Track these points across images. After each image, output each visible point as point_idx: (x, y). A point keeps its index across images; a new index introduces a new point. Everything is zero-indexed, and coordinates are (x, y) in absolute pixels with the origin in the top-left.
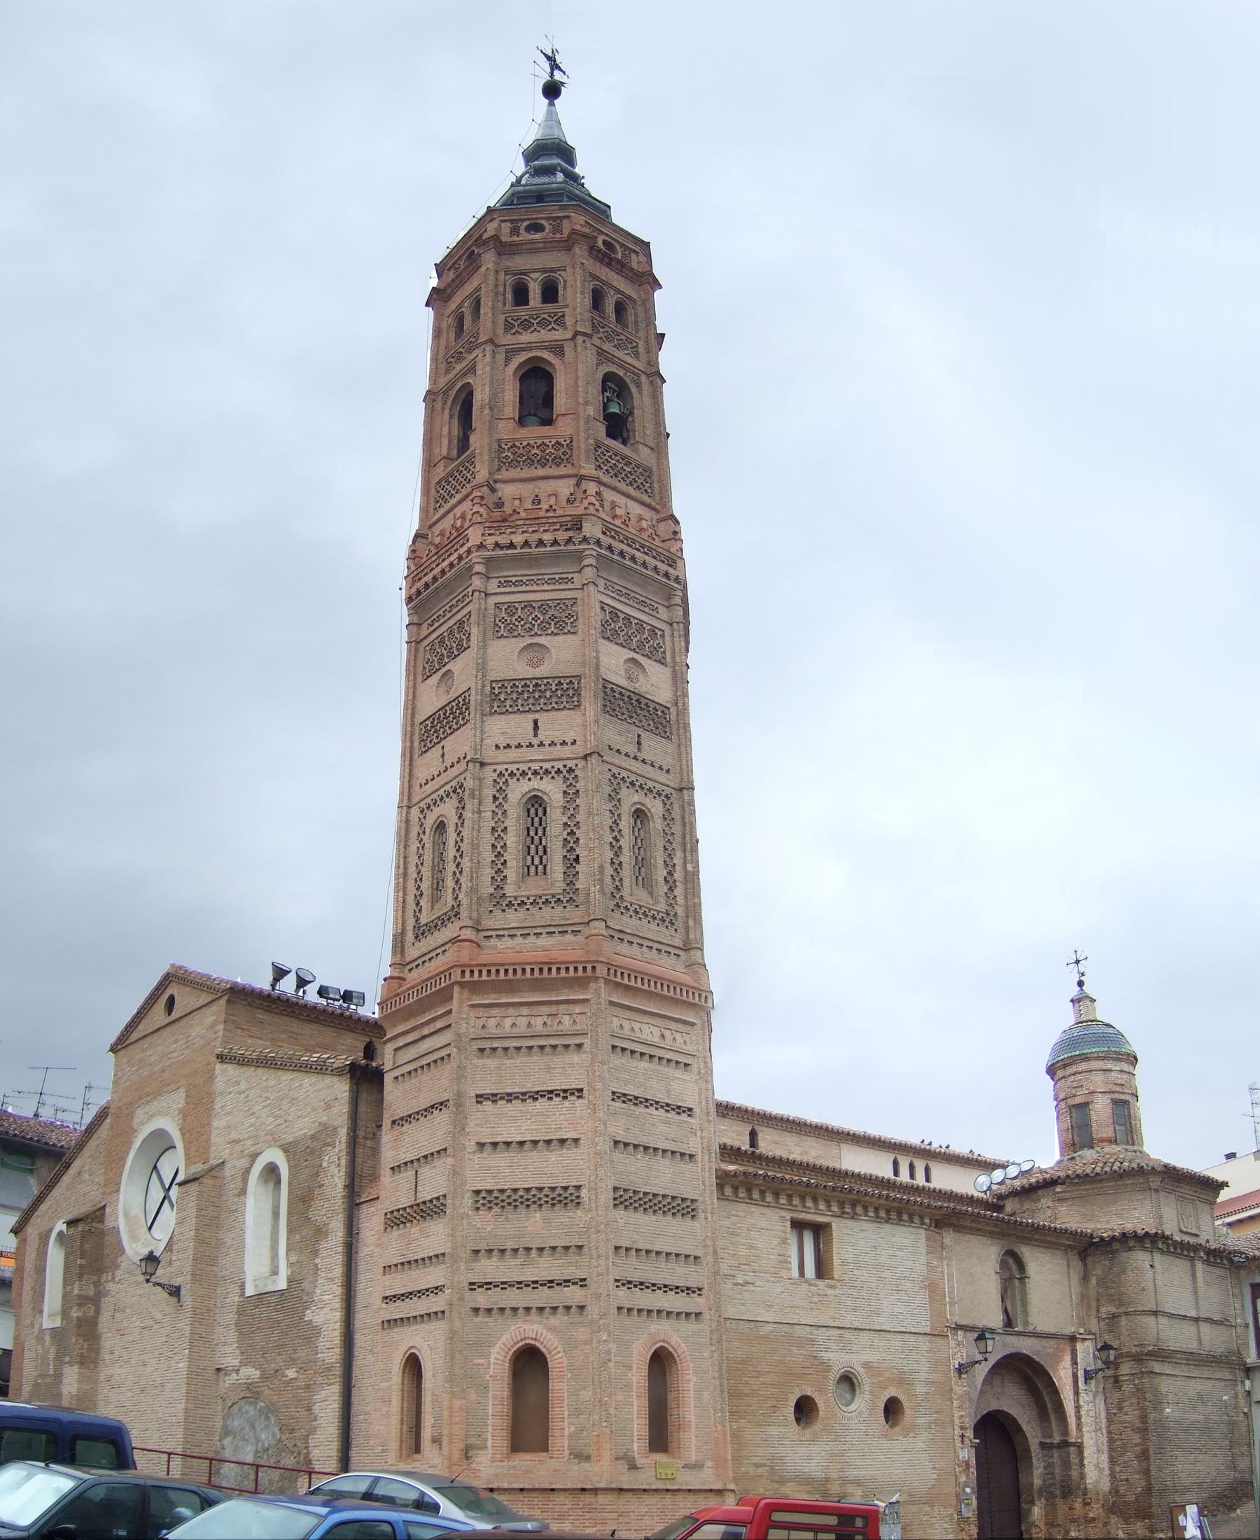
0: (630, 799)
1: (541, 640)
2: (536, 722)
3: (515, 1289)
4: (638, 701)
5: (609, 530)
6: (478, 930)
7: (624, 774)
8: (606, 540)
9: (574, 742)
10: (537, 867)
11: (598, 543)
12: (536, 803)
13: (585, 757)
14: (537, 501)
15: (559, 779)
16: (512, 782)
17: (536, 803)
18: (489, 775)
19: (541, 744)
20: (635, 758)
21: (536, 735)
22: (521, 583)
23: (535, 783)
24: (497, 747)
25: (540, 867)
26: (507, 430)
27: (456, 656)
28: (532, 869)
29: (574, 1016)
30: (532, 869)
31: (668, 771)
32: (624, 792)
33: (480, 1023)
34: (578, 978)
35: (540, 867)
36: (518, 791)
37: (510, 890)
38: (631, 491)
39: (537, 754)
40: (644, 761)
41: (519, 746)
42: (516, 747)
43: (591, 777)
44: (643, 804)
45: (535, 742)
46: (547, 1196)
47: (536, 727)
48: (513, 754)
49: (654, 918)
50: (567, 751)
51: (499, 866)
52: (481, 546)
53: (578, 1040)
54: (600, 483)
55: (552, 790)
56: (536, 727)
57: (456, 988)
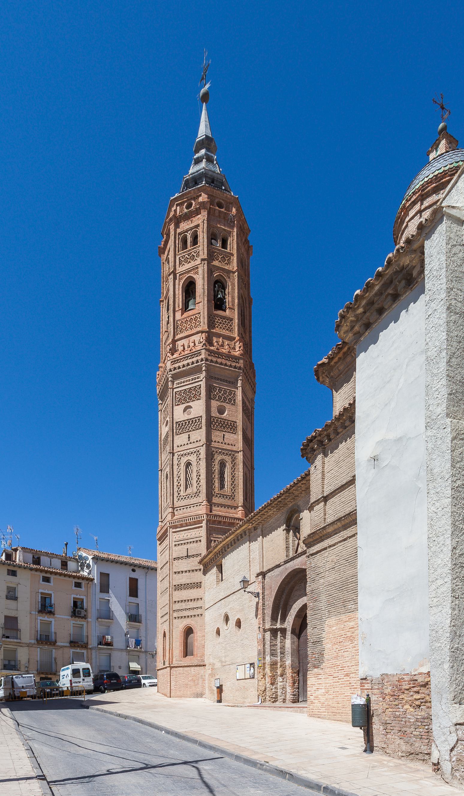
9: (200, 441)
10: (190, 485)
13: (202, 446)
25: (191, 485)
28: (188, 486)
35: (191, 485)
36: (184, 460)
37: (182, 493)
55: (193, 458)
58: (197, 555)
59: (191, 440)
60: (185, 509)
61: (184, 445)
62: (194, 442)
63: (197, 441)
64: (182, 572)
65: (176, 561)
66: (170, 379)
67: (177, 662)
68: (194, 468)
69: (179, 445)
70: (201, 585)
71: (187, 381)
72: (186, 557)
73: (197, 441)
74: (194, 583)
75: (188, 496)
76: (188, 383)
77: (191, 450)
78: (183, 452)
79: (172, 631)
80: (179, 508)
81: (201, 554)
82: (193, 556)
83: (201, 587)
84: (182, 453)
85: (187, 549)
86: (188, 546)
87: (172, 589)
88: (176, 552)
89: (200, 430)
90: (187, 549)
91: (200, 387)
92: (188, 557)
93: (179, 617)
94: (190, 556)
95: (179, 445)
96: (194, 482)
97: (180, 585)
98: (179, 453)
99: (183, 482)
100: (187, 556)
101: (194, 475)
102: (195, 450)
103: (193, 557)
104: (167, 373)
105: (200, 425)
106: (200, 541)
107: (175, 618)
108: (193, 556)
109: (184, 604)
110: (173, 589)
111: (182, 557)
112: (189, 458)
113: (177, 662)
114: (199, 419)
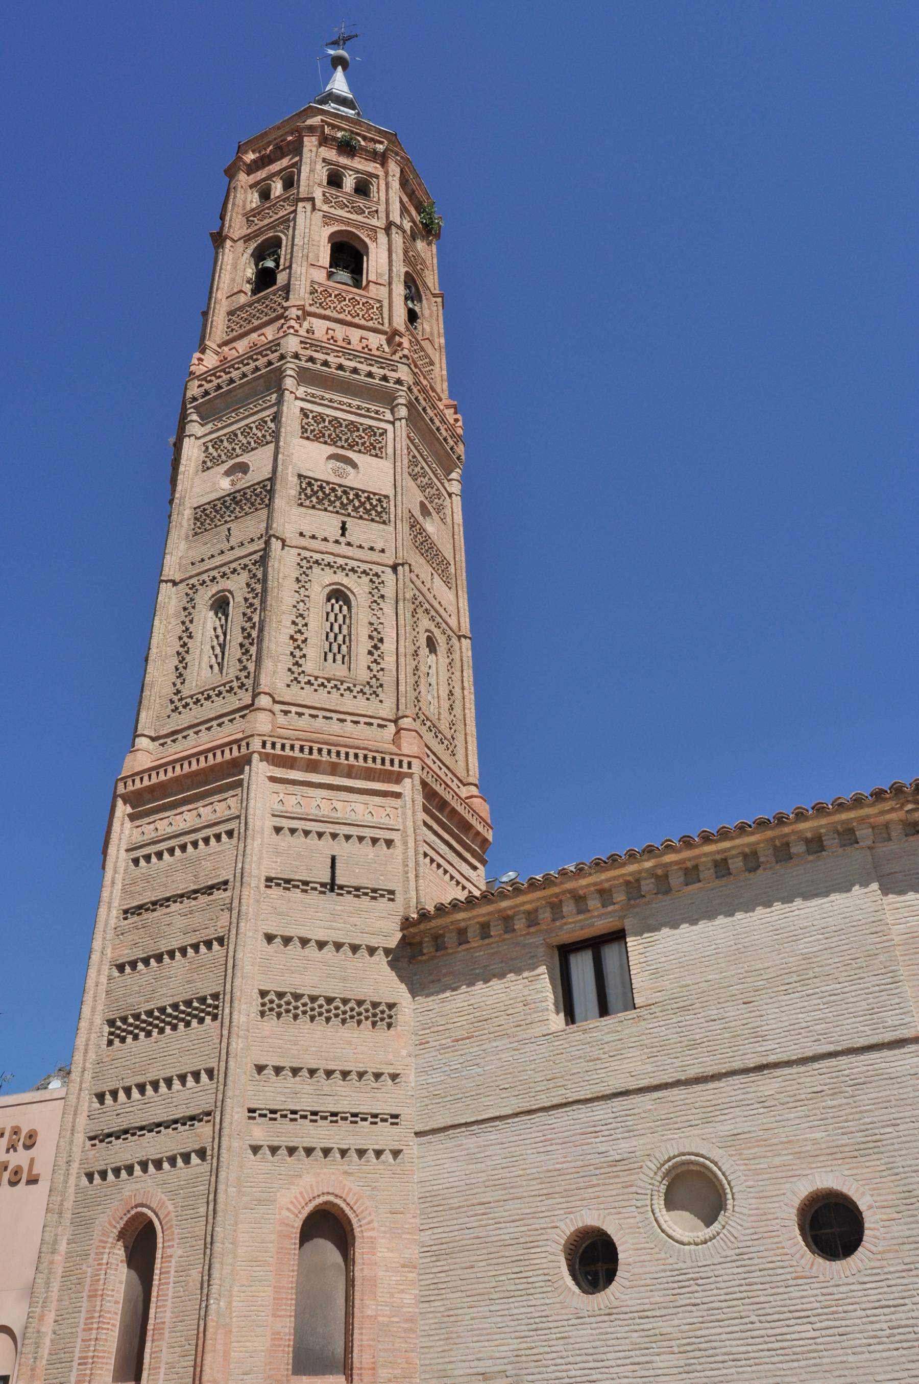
3: (308, 1121)
6: (275, 702)
9: (383, 551)
11: (409, 389)
15: (365, 579)
16: (316, 570)
21: (343, 535)
23: (340, 577)
24: (301, 534)
27: (253, 449)
39: (343, 549)
41: (325, 540)
42: (322, 540)
45: (342, 540)
46: (337, 1008)
47: (344, 528)
50: (374, 557)
59: (349, 537)
64: (304, 942)
65: (276, 892)
72: (323, 885)
82: (357, 891)
85: (333, 859)
86: (341, 849)
90: (333, 859)
92: (332, 890)
93: (274, 1150)
94: (341, 887)
100: (332, 886)
107: (255, 1149)
108: (357, 891)
109: (308, 1088)
111: (306, 883)
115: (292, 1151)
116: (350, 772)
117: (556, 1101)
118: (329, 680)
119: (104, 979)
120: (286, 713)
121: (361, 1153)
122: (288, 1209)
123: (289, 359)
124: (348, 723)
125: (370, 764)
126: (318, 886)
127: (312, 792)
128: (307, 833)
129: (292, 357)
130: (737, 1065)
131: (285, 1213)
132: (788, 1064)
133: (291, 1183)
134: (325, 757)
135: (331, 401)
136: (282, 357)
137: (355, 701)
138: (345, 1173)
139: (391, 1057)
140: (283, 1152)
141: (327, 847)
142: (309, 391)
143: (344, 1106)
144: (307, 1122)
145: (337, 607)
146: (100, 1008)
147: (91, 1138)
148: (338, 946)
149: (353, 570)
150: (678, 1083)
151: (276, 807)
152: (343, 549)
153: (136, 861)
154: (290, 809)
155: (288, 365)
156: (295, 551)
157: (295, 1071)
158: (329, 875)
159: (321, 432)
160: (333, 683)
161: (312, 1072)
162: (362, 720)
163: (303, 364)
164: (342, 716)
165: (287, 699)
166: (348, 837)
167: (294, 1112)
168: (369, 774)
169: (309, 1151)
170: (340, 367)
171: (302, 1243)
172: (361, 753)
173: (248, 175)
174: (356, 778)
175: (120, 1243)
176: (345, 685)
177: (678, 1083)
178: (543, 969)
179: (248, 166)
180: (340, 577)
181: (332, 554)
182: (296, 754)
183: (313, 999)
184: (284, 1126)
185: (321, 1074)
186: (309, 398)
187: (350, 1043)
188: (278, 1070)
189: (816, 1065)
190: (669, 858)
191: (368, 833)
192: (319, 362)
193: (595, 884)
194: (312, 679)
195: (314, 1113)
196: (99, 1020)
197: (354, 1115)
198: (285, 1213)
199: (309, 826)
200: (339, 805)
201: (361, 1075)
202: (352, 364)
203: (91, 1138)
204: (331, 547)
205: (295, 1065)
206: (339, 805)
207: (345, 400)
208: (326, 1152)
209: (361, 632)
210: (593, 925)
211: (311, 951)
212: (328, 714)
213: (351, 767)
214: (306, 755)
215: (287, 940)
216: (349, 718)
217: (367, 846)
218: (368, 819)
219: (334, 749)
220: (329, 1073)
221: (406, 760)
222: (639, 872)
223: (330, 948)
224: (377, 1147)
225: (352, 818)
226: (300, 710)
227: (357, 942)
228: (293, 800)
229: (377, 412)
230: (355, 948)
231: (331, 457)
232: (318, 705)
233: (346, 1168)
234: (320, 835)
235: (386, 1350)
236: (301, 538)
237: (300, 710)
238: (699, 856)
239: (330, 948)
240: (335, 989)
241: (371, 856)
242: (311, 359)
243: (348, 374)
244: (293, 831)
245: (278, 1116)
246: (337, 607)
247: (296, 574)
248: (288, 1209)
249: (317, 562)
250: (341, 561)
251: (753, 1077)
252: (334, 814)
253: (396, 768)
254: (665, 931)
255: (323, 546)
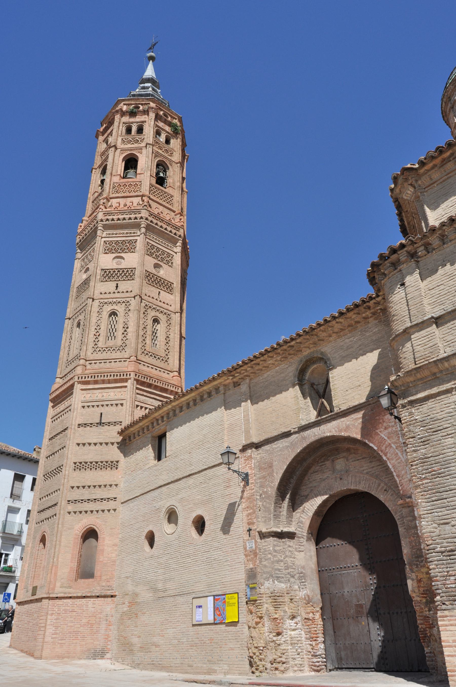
0: (152, 314)
1: (122, 255)
2: (117, 284)
4: (160, 280)
5: (152, 215)
6: (86, 360)
7: (151, 305)
8: (150, 218)
9: (131, 291)
11: (147, 219)
12: (113, 314)
13: (134, 297)
14: (125, 205)
17: (113, 314)
18: (96, 303)
19: (119, 292)
20: (156, 299)
21: (117, 289)
22: (116, 234)
24: (101, 293)
26: (116, 179)
28: (110, 338)
29: (122, 392)
30: (110, 338)
31: (171, 306)
32: (149, 310)
33: (83, 396)
34: (123, 379)
35: (113, 337)
36: (108, 309)
38: (164, 203)
39: (117, 295)
40: (160, 301)
43: (134, 303)
44: (157, 316)
47: (117, 287)
48: (107, 296)
49: (159, 358)
51: (97, 336)
52: (102, 220)
53: (121, 402)
54: (150, 199)
55: (120, 309)
56: (117, 287)
57: (76, 383)
58: (115, 423)
59: (119, 289)
60: (103, 364)
61: (110, 293)
62: (123, 292)
63: (127, 292)
64: (90, 444)
65: (82, 428)
66: (99, 228)
67: (61, 590)
68: (121, 319)
69: (103, 293)
70: (117, 465)
71: (120, 234)
72: (97, 424)
73: (127, 292)
74: (107, 462)
75: (108, 349)
76: (121, 235)
77: (119, 300)
78: (108, 300)
79: (61, 536)
80: (93, 362)
81: (121, 422)
82: (109, 424)
83: (117, 468)
84: (106, 301)
85: (101, 414)
86: (104, 410)
87: (70, 467)
88: (82, 415)
89: (131, 281)
90: (101, 414)
91: (136, 242)
92: (100, 425)
93: (75, 512)
94: (103, 423)
95: (103, 293)
96: (119, 335)
97: (85, 462)
98: (102, 301)
99: (103, 332)
100: (101, 423)
101: (120, 327)
102: (124, 300)
103: (109, 426)
104: (97, 222)
105: (133, 276)
106: (122, 405)
107: (69, 513)
108: (109, 424)
109: (87, 492)
110: (71, 469)
111: (91, 424)
112: (115, 307)
113: (61, 590)
114: (132, 271)
115: (81, 512)
116: (109, 382)
117: (148, 490)
118: (107, 348)
119: (43, 462)
120: (90, 364)
121: (103, 511)
122: (78, 530)
123: (99, 223)
124: (113, 363)
125: (115, 377)
126: (96, 424)
127: (95, 391)
128: (93, 406)
129: (100, 221)
130: (185, 475)
131: (77, 532)
132: (196, 473)
133: (79, 522)
134: (99, 378)
135: (116, 234)
136: (97, 222)
137: (116, 354)
138: (97, 518)
139: (115, 479)
140: (78, 513)
141: (98, 411)
142: (108, 232)
143: (98, 496)
144: (86, 503)
145: (114, 318)
146: (42, 471)
147: (38, 512)
148: (101, 444)
149: (119, 302)
150: (172, 482)
151: (83, 399)
152: (117, 295)
153: (52, 422)
154: (87, 399)
155: (99, 225)
156: (97, 301)
157: (84, 487)
158: (99, 420)
159: (111, 249)
160: (108, 348)
161: (89, 487)
162: (118, 360)
163: (104, 223)
164: (110, 360)
165: (91, 358)
166: (107, 405)
167: (82, 500)
168: (116, 381)
169: (86, 512)
170: (119, 219)
171: (84, 541)
172: (112, 374)
173: (103, 136)
174: (112, 383)
175: (41, 543)
176: (113, 349)
177: (172, 482)
178: (150, 445)
179: (102, 132)
180: (115, 307)
181: (111, 298)
182: (90, 379)
183: (91, 463)
184: (79, 505)
185: (92, 487)
186: (108, 236)
187: (102, 476)
188: (78, 487)
189: (202, 473)
190: (174, 404)
191: (114, 402)
192: (110, 220)
193: (160, 415)
194: (101, 349)
195: (88, 500)
196: (42, 476)
197: (102, 499)
198: (77, 532)
199: (88, 404)
200: (105, 394)
201: (105, 486)
202: (123, 217)
203: (38, 512)
204: (112, 295)
205: (83, 485)
206: (105, 394)
207: (122, 232)
208: (92, 512)
209: (120, 327)
210: (161, 429)
211: (92, 447)
212: (105, 361)
213: (109, 380)
214: (93, 379)
215: (84, 444)
216: (113, 361)
217: (114, 408)
218: (116, 397)
219: (103, 375)
220: (95, 487)
221: (128, 373)
222: (169, 410)
223: (98, 445)
224: (108, 509)
225: (110, 398)
226: (95, 362)
227: (107, 442)
228: (89, 395)
229: (134, 233)
230: (107, 444)
231: (114, 258)
232: (102, 358)
233: (97, 516)
234: (98, 406)
235: (105, 571)
236: (101, 295)
237: (95, 362)
238: (182, 402)
239: (98, 445)
240: (98, 459)
241: (115, 410)
242: (107, 220)
243: (121, 221)
244: (88, 406)
245: (77, 502)
246: (114, 318)
247: (98, 310)
248: (78, 530)
249: (106, 303)
250: (115, 300)
251: (188, 478)
252: (103, 398)
253: (125, 377)
254: (175, 429)
255: (107, 296)
